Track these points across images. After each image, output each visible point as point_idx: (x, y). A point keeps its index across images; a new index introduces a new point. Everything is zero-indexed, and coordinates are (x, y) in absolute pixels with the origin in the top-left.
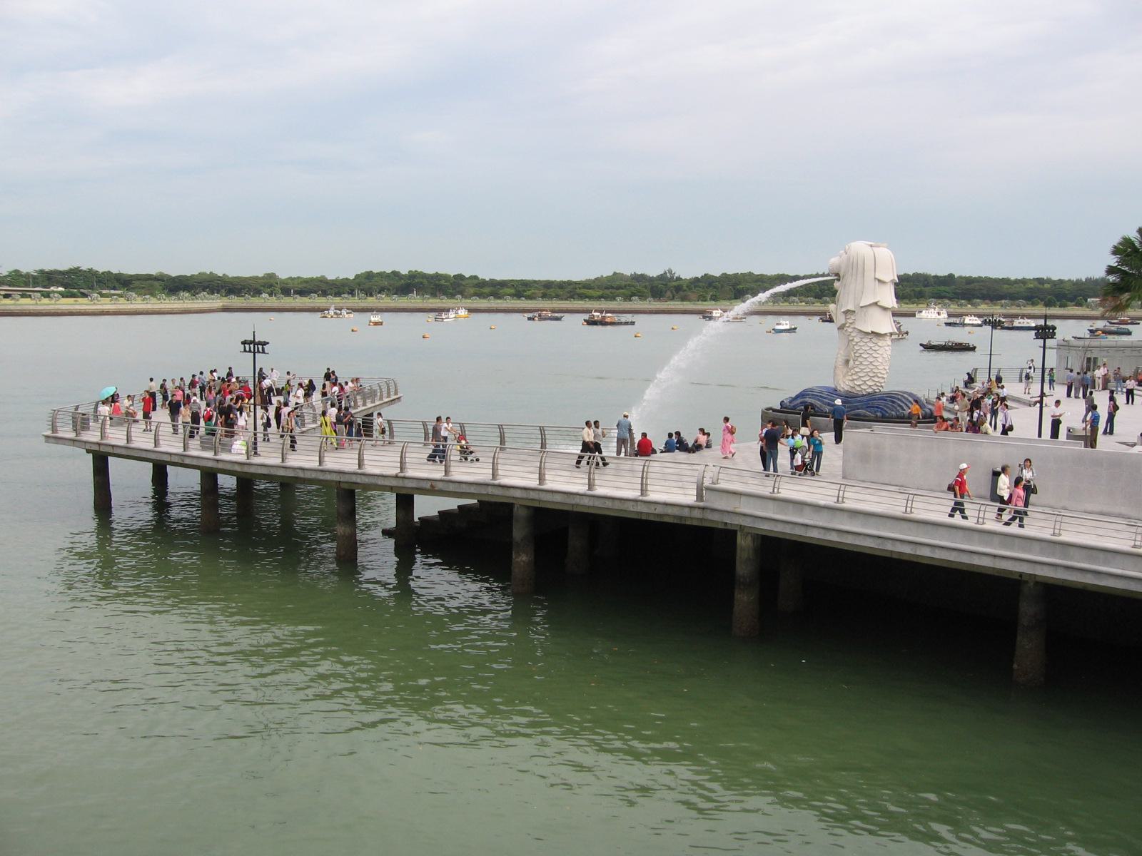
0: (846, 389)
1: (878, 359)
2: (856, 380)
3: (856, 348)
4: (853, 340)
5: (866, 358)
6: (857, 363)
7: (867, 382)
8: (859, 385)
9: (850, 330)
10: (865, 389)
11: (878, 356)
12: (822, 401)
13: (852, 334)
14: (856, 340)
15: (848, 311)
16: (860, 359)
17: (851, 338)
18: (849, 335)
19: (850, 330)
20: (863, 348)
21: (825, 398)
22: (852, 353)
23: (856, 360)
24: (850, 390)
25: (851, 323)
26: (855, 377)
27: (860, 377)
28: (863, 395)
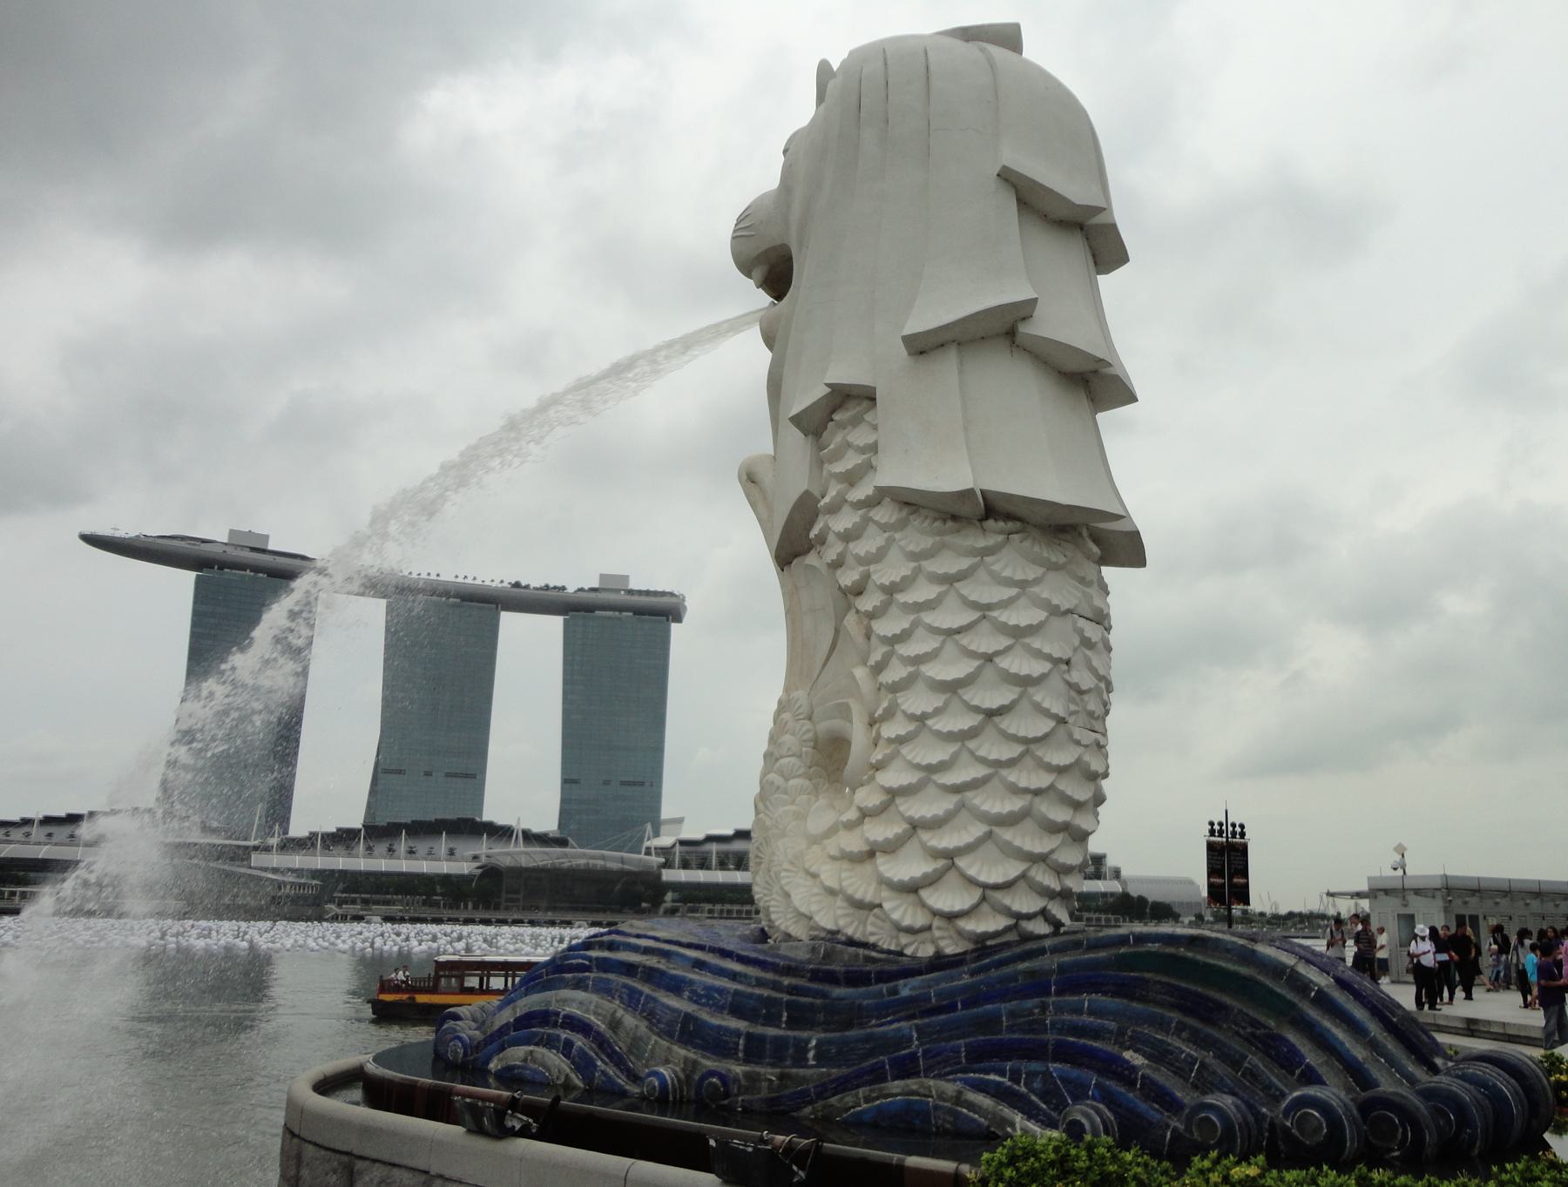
0: (826, 921)
1: (1039, 695)
2: (891, 848)
3: (886, 627)
4: (859, 590)
6: (890, 730)
7: (967, 864)
8: (911, 889)
9: (843, 522)
10: (951, 917)
11: (1037, 668)
12: (650, 1014)
13: (862, 547)
14: (886, 574)
16: (918, 701)
17: (848, 578)
18: (837, 565)
19: (843, 522)
21: (676, 986)
22: (860, 673)
23: (889, 714)
24: (852, 928)
25: (851, 479)
26: (879, 831)
27: (915, 826)
28: (940, 962)
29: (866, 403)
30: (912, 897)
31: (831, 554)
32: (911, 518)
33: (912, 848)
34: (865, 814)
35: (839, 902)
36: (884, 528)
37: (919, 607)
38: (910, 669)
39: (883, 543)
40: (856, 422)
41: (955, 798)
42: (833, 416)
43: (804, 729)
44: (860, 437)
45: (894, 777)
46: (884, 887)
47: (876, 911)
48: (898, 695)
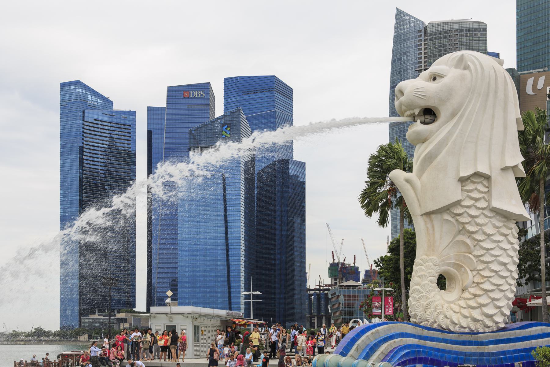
5: (505, 264)
8: (490, 317)
9: (473, 212)
10: (497, 323)
13: (479, 220)
15: (477, 174)
20: (501, 245)
25: (477, 200)
27: (494, 299)
29: (483, 178)
30: (490, 319)
31: (464, 219)
32: (496, 216)
33: (491, 305)
34: (475, 296)
35: (469, 319)
36: (487, 216)
37: (499, 242)
38: (495, 258)
39: (487, 222)
40: (481, 182)
41: (503, 293)
43: (437, 269)
44: (481, 187)
45: (487, 286)
46: (483, 316)
47: (481, 322)
48: (489, 264)
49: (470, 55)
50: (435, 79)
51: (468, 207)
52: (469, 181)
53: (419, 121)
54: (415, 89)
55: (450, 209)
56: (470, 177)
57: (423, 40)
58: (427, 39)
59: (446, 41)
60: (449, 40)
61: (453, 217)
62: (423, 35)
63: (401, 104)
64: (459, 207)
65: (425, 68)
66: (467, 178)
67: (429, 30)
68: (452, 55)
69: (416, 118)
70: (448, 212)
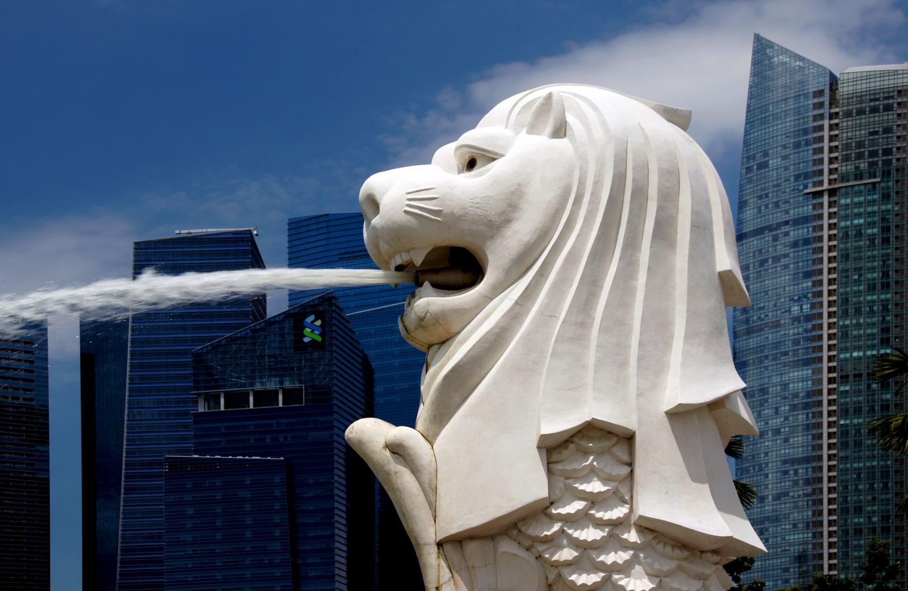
25: (594, 500)
32: (654, 542)
42: (576, 439)
49: (575, 95)
50: (471, 164)
51: (568, 520)
52: (572, 446)
53: (427, 284)
54: (408, 193)
55: (519, 525)
56: (572, 436)
57: (827, 115)
58: (837, 113)
59: (891, 117)
60: (899, 115)
61: (528, 549)
62: (827, 103)
63: (377, 237)
64: (545, 519)
65: (831, 187)
66: (565, 437)
67: (844, 90)
68: (524, 97)
69: (421, 278)
70: (515, 532)
